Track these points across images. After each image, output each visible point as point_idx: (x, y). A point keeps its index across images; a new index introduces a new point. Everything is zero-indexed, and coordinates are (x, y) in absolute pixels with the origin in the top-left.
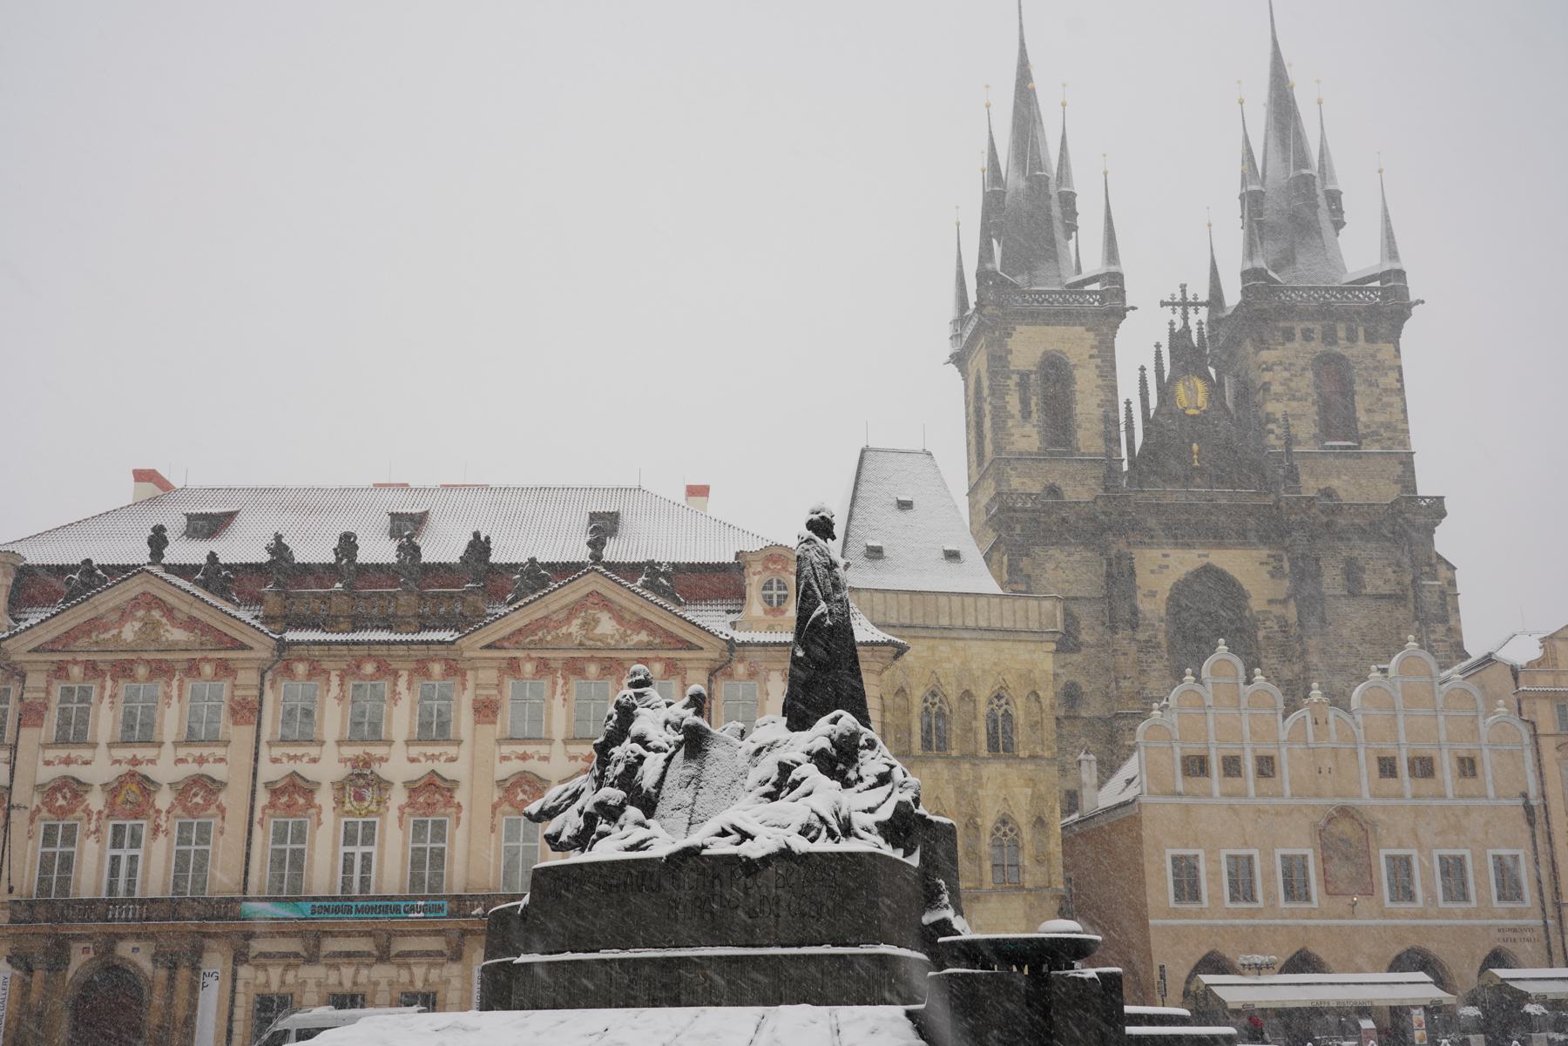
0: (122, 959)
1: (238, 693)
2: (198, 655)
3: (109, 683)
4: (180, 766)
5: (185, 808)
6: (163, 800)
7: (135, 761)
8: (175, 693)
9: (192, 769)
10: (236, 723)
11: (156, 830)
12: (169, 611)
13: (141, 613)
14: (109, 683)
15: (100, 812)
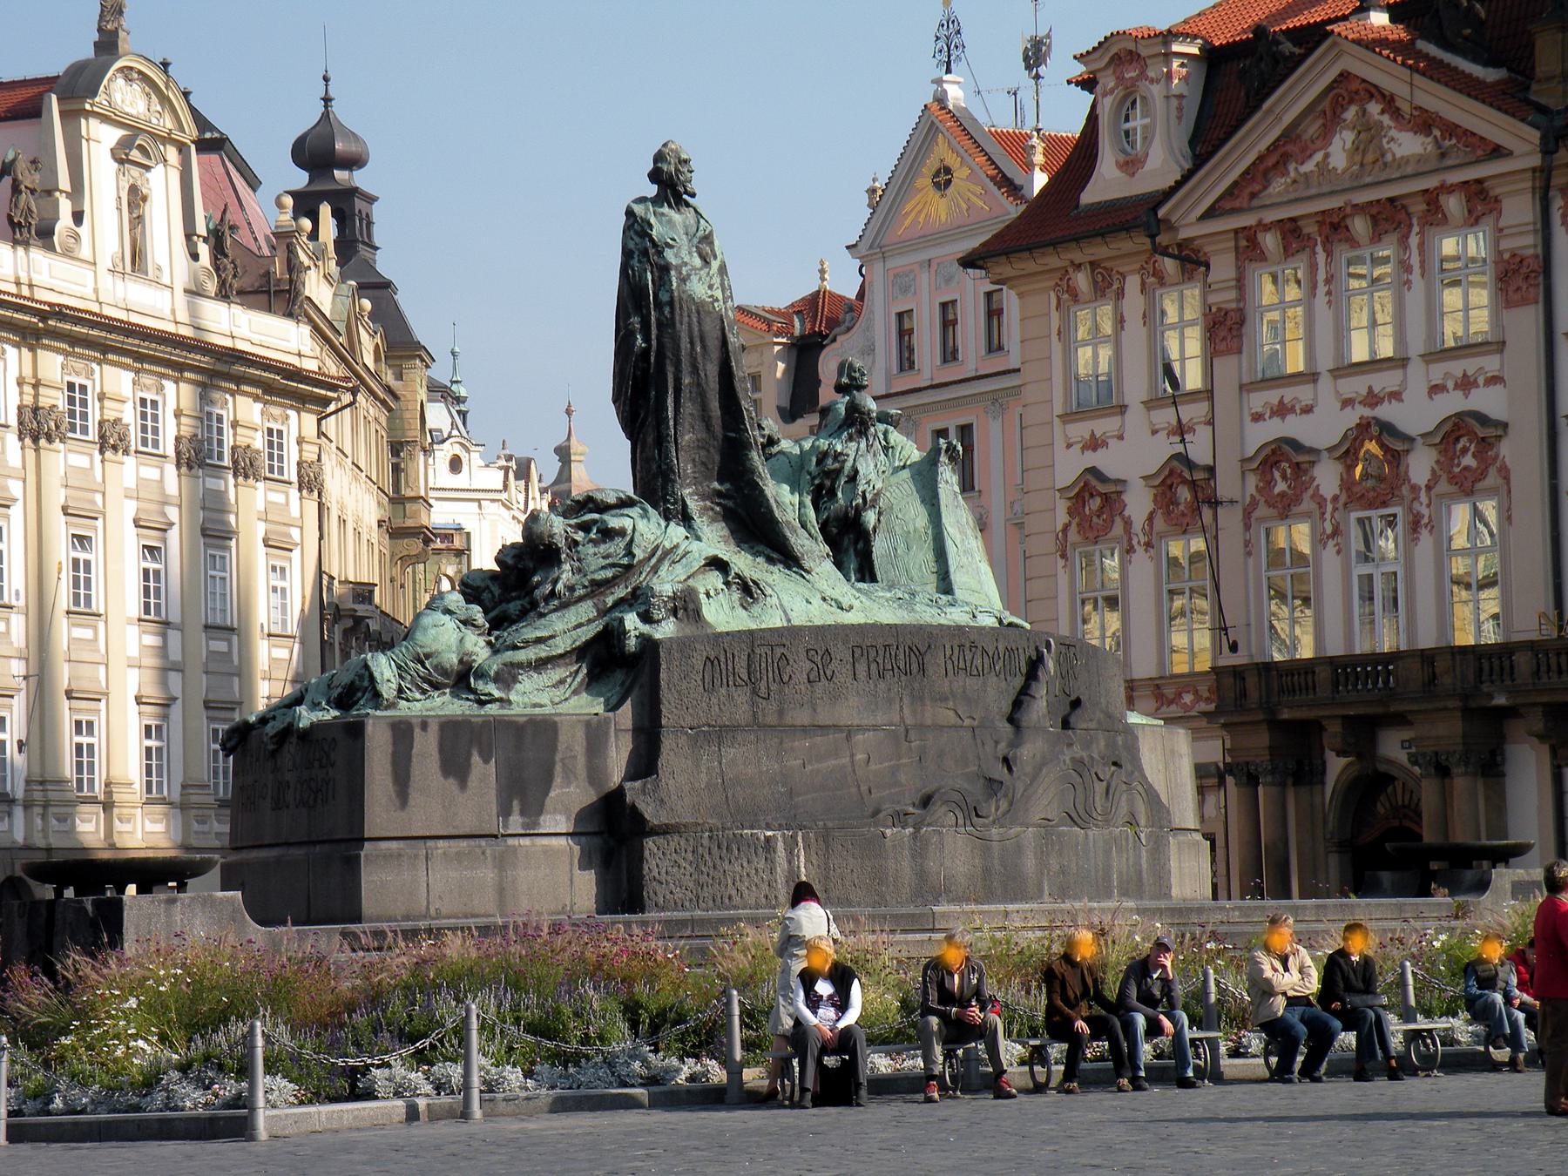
0: (1390, 762)
1: (1506, 244)
2: (1431, 183)
3: (1321, 257)
4: (1438, 397)
5: (1452, 479)
6: (1420, 465)
7: (1372, 399)
8: (1415, 261)
9: (1454, 403)
10: (1509, 304)
11: (1415, 525)
12: (1389, 102)
13: (1351, 113)
14: (1321, 257)
15: (1335, 499)
